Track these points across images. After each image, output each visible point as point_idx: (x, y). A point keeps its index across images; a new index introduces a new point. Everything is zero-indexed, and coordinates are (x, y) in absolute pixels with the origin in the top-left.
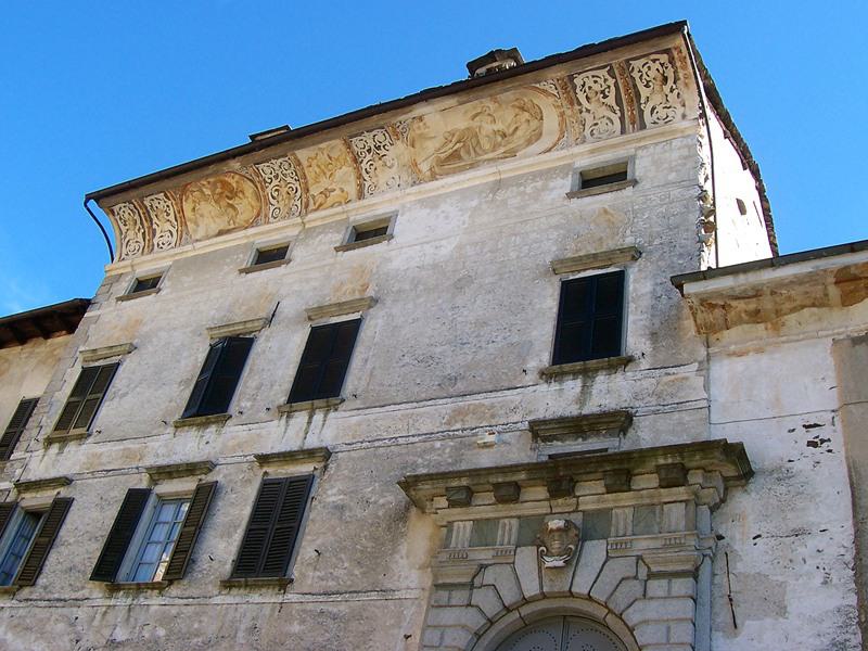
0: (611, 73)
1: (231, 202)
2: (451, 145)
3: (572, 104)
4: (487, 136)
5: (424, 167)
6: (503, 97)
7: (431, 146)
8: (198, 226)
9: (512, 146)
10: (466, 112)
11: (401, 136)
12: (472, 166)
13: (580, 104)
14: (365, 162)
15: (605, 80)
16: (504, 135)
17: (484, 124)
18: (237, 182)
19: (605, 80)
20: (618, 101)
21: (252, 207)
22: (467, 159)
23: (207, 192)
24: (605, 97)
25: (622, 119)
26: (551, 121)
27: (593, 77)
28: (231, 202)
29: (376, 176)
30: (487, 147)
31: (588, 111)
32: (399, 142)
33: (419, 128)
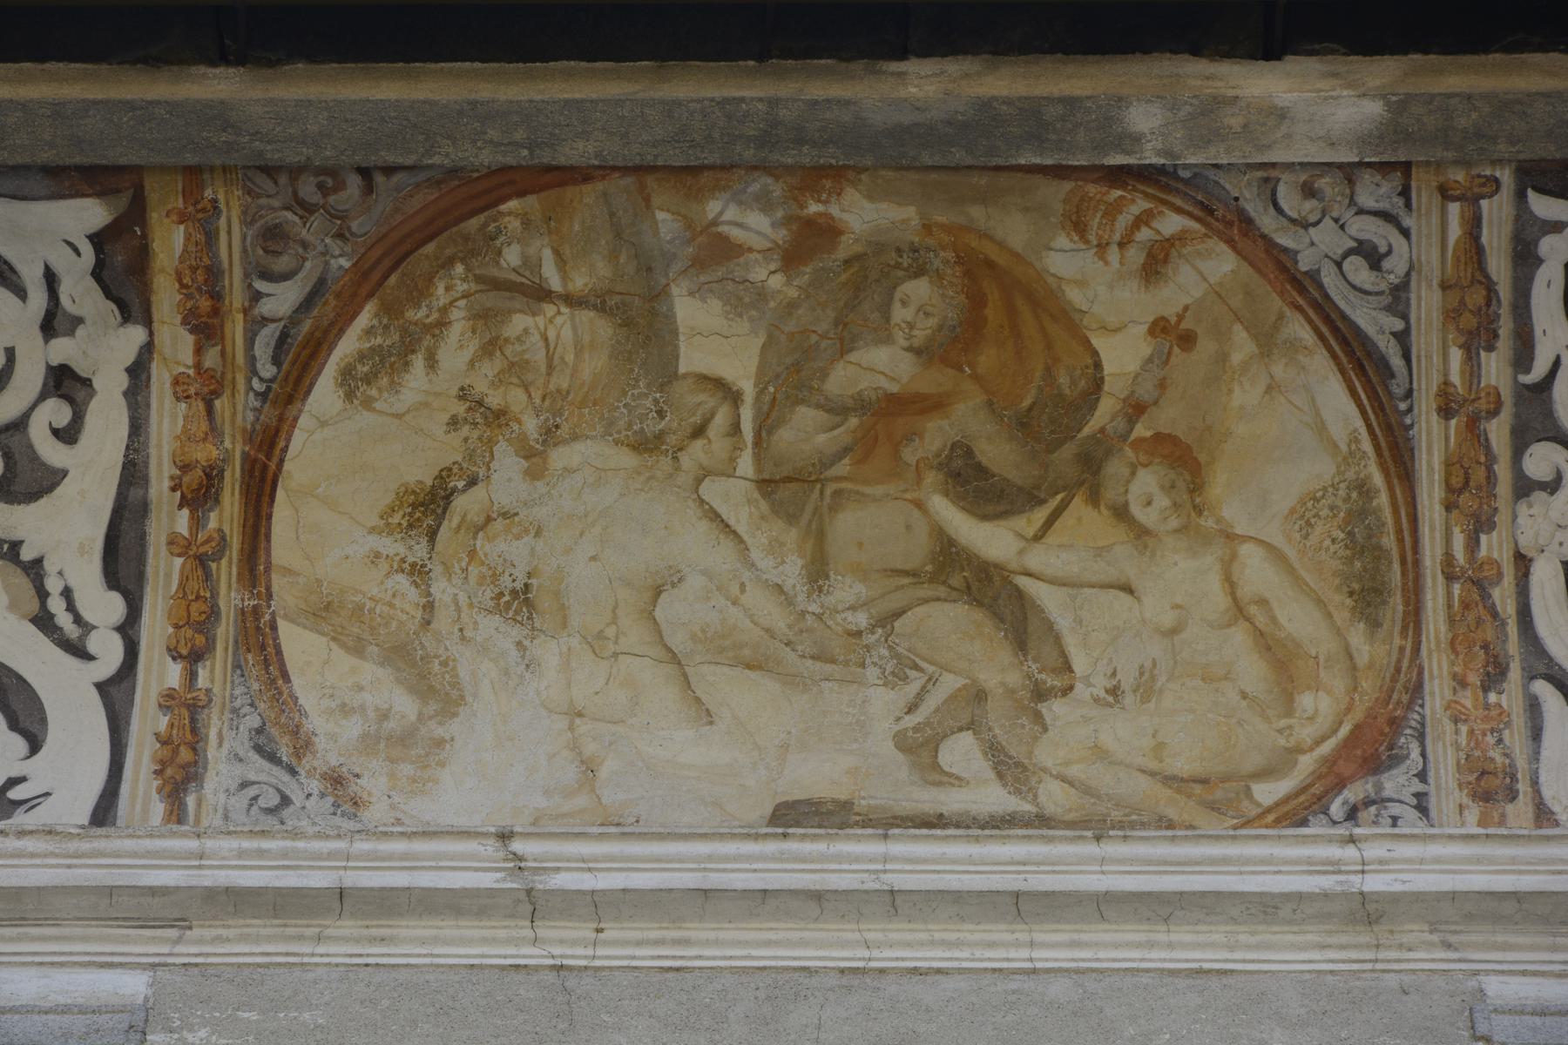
1: (992, 540)
8: (440, 693)
18: (1173, 334)
21: (1285, 663)
23: (715, 340)
28: (992, 540)
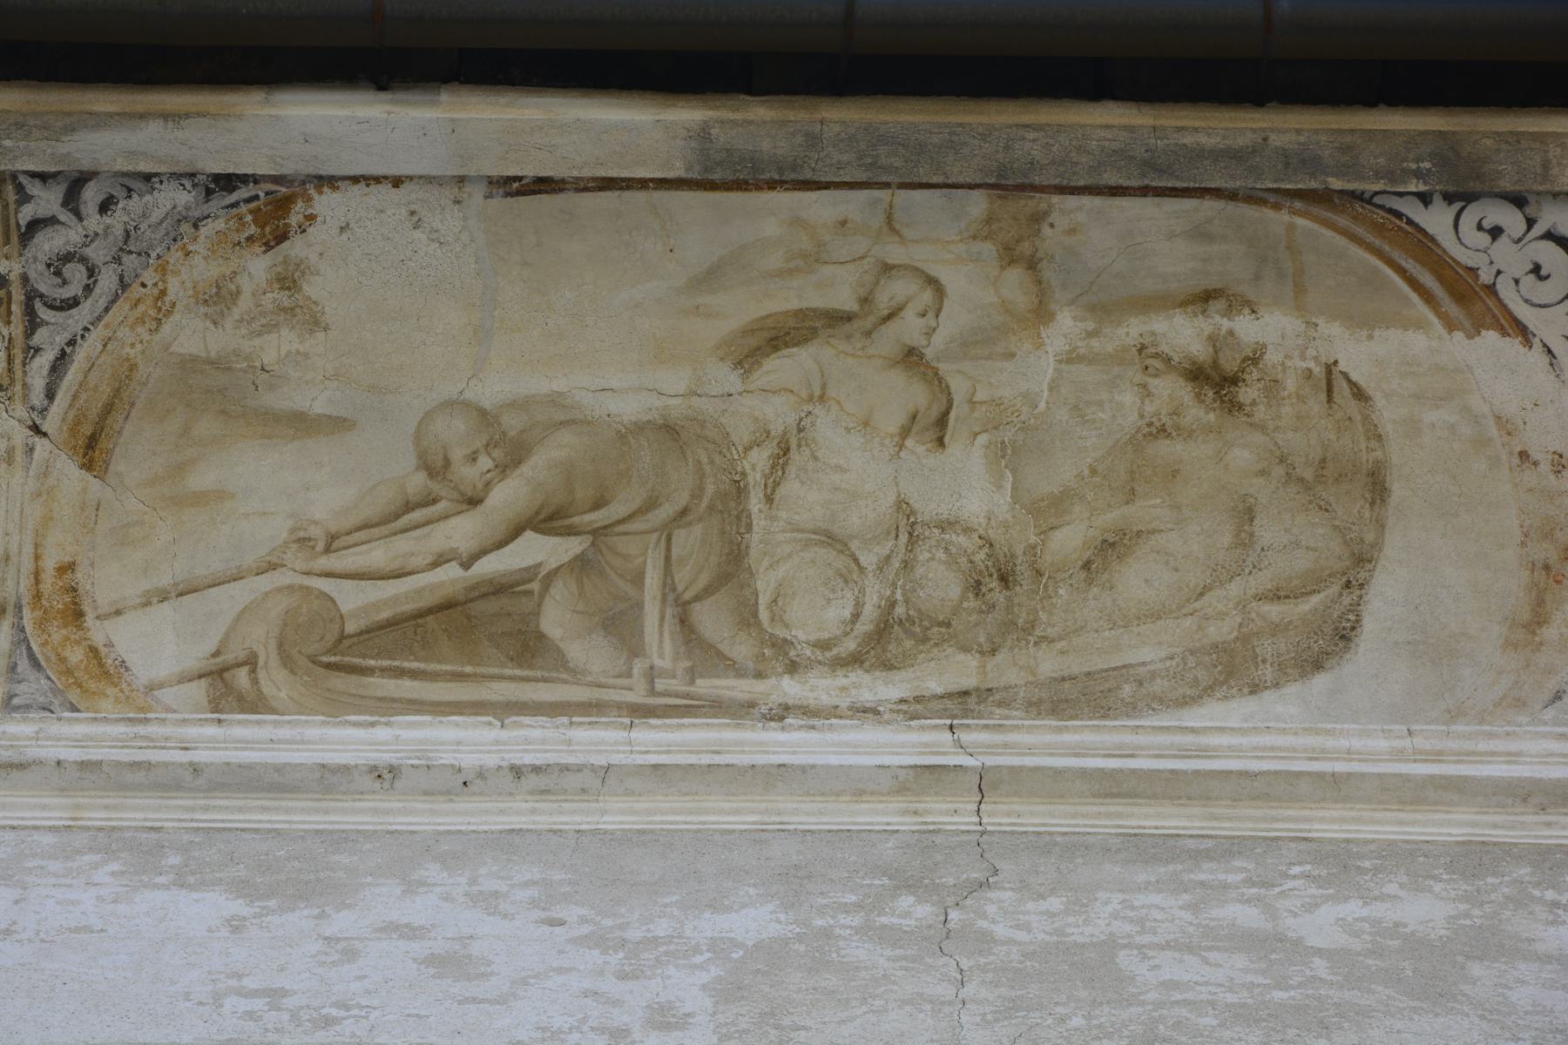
2: (462, 531)
4: (831, 539)
6: (1091, 230)
10: (709, 278)
17: (825, 427)
30: (819, 612)
33: (218, 298)
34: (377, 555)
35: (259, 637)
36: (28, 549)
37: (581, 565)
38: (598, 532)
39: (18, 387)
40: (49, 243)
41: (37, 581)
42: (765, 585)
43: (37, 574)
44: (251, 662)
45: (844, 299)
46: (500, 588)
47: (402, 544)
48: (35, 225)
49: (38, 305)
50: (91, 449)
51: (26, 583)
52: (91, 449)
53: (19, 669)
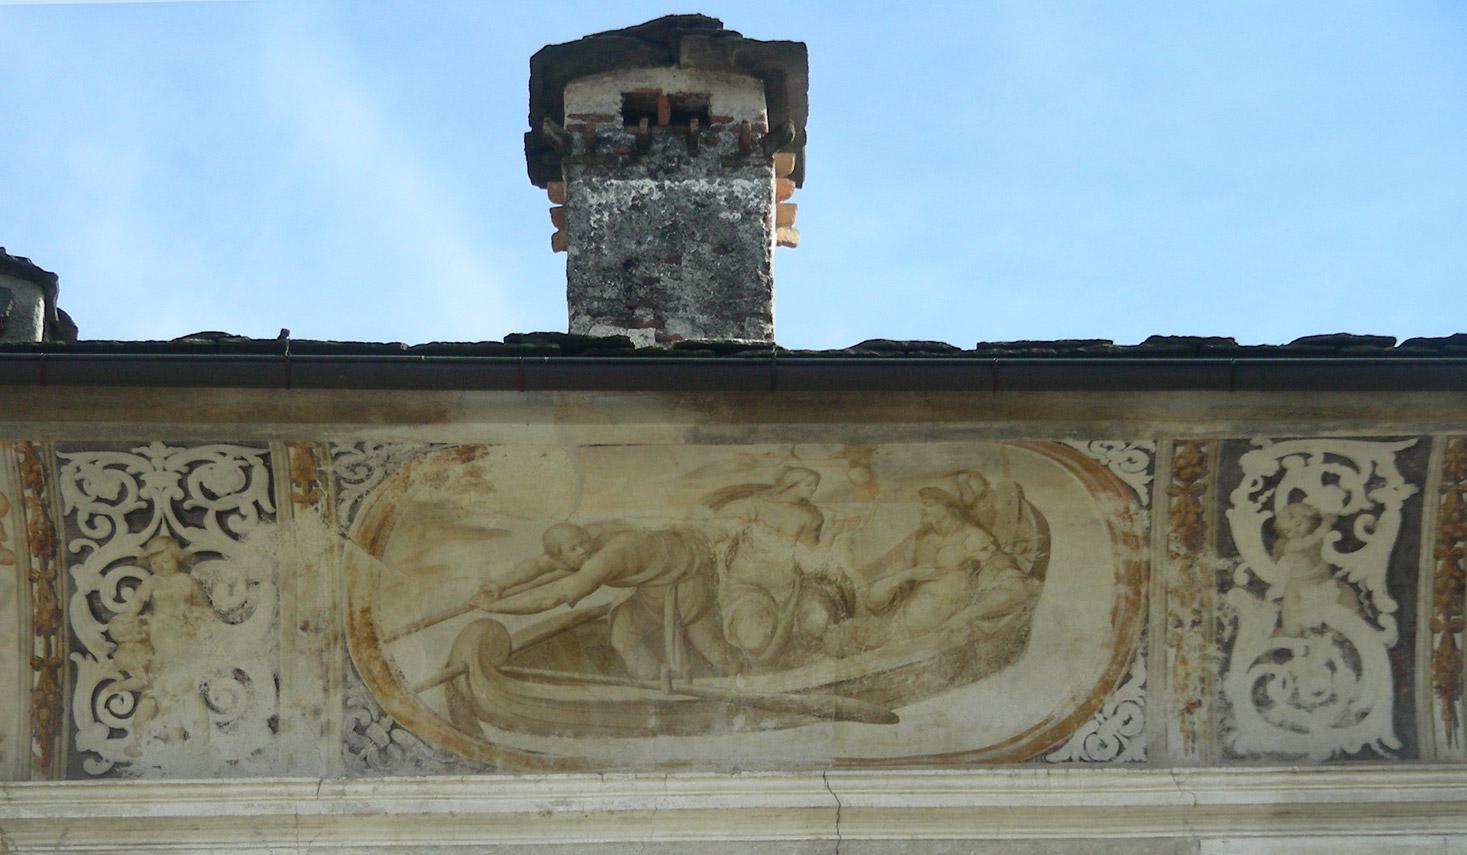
0: (1411, 464)
2: (568, 585)
3: (1193, 539)
4: (761, 588)
5: (417, 661)
7: (467, 567)
9: (871, 663)
10: (699, 472)
11: (325, 493)
12: (675, 716)
13: (1228, 548)
14: (99, 557)
15: (1375, 481)
16: (844, 605)
17: (757, 532)
19: (1375, 481)
20: (1401, 574)
22: (645, 676)
24: (1348, 544)
25: (1401, 658)
26: (1080, 592)
27: (1329, 458)
29: (146, 641)
30: (751, 635)
31: (1257, 586)
32: (307, 521)
33: (438, 479)
34: (525, 600)
35: (468, 655)
36: (345, 600)
37: (632, 604)
38: (640, 585)
39: (334, 516)
40: (345, 460)
41: (352, 619)
42: (726, 613)
43: (351, 615)
44: (466, 671)
45: (767, 478)
46: (589, 618)
47: (539, 593)
48: (338, 455)
49: (342, 482)
50: (374, 544)
51: (346, 619)
52: (374, 544)
53: (349, 679)
